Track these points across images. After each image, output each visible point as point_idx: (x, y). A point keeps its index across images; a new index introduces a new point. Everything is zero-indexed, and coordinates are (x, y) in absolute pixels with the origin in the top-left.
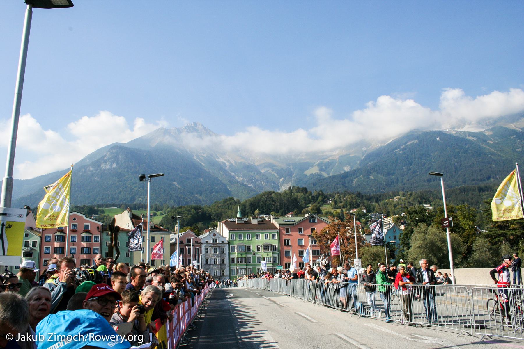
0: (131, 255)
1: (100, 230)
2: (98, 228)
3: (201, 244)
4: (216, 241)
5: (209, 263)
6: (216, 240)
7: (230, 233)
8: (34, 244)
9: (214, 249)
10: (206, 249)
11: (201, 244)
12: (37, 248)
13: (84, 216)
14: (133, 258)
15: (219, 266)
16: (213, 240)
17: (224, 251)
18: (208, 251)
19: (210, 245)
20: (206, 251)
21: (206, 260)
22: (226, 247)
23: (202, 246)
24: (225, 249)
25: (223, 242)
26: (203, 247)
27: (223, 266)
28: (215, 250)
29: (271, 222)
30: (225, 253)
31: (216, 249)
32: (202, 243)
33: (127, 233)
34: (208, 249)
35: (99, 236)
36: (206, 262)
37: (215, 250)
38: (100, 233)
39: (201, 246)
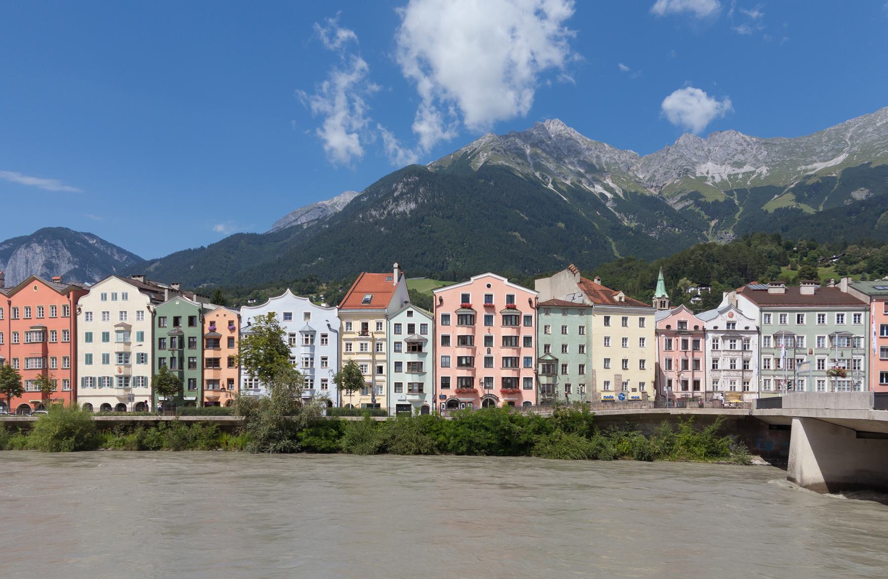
0: (587, 349)
1: (534, 306)
2: (530, 302)
3: (704, 332)
4: (733, 327)
6: (734, 324)
7: (761, 311)
8: (424, 326)
9: (731, 341)
12: (429, 336)
13: (506, 280)
14: (591, 355)
15: (741, 373)
16: (728, 324)
18: (717, 345)
20: (714, 345)
21: (713, 361)
24: (751, 341)
25: (747, 328)
26: (710, 336)
27: (747, 374)
28: (715, 343)
30: (750, 349)
31: (735, 341)
33: (579, 310)
34: (717, 342)
36: (713, 365)
37: (715, 343)
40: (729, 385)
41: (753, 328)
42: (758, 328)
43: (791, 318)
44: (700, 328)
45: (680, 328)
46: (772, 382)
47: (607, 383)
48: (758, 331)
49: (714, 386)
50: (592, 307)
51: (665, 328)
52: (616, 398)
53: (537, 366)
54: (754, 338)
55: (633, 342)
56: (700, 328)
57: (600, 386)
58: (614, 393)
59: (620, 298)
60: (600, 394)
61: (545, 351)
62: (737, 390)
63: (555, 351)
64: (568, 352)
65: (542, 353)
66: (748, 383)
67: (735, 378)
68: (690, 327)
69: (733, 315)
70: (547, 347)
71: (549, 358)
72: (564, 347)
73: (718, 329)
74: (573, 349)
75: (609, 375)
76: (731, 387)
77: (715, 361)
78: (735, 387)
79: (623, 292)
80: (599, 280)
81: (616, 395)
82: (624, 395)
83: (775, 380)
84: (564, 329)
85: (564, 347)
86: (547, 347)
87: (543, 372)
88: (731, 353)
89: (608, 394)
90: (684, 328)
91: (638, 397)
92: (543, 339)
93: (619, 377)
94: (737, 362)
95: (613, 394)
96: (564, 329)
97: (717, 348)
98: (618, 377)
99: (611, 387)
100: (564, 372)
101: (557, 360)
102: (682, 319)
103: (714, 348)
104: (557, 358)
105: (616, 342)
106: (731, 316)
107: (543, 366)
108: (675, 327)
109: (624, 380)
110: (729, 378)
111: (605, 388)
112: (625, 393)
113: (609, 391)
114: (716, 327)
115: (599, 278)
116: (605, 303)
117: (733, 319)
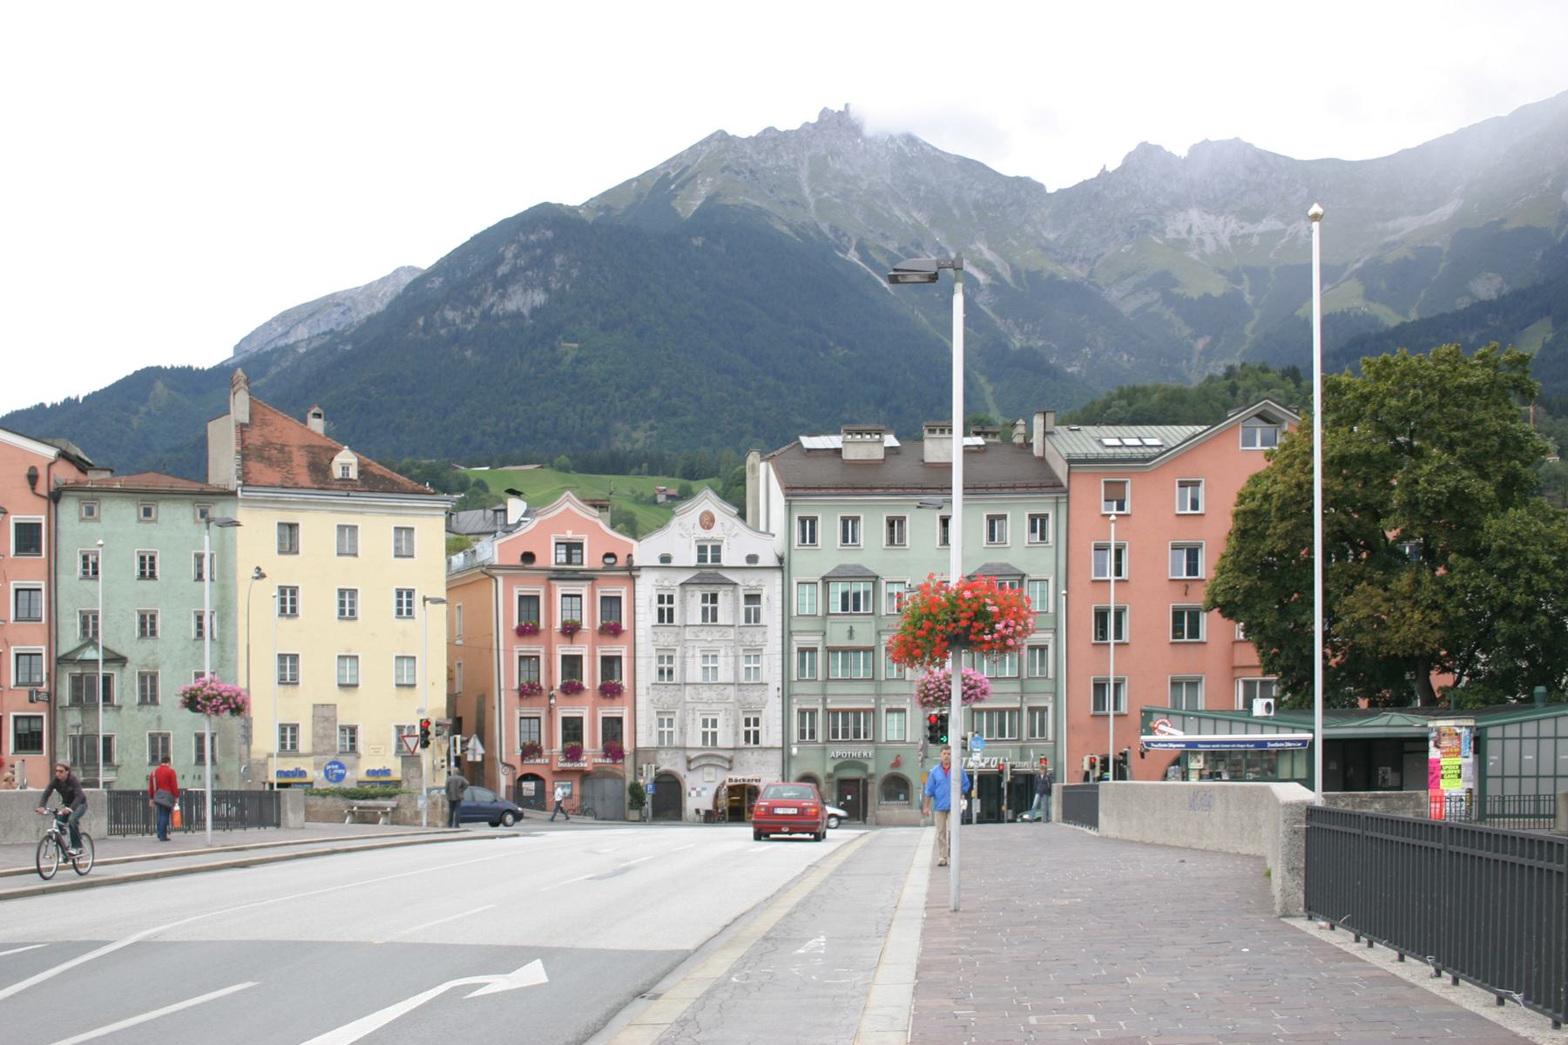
3: (631, 571)
4: (716, 558)
5: (676, 677)
6: (717, 549)
10: (661, 599)
11: (631, 571)
16: (702, 549)
17: (757, 612)
18: (671, 611)
19: (686, 576)
20: (661, 611)
22: (771, 588)
23: (638, 581)
24: (763, 599)
25: (752, 558)
29: (1037, 451)
30: (763, 621)
31: (714, 598)
32: (639, 568)
35: (43, 520)
38: (45, 502)
39: (633, 578)
40: (700, 729)
41: (768, 559)
42: (781, 559)
43: (872, 528)
44: (622, 562)
45: (562, 558)
46: (820, 716)
47: (288, 733)
48: (782, 564)
49: (661, 733)
50: (234, 493)
51: (517, 560)
52: (315, 775)
53: (53, 678)
54: (771, 588)
55: (376, 604)
56: (622, 562)
57: (265, 740)
58: (311, 760)
59: (345, 468)
60: (264, 765)
61: (85, 633)
62: (720, 743)
63: (118, 633)
64: (159, 634)
65: (70, 639)
66: (757, 722)
67: (715, 707)
68: (590, 559)
69: (713, 520)
70: (89, 622)
71: (90, 654)
72: (147, 626)
73: (671, 564)
74: (174, 625)
75: (298, 708)
76: (705, 734)
77: (665, 656)
78: (714, 734)
79: (352, 449)
80: (319, 416)
81: (317, 766)
82: (341, 766)
83: (828, 711)
84: (147, 569)
85: (147, 626)
86: (89, 622)
87: (77, 700)
88: (703, 636)
89: (290, 765)
90: (575, 559)
91: (386, 772)
92: (74, 593)
93: (327, 713)
94: (721, 660)
95: (306, 765)
96: (147, 569)
97: (671, 619)
98: (324, 713)
99: (305, 744)
100: (149, 696)
101: (120, 660)
102: (570, 535)
103: (661, 619)
104: (124, 653)
105: (317, 603)
106: (708, 521)
107: (76, 681)
108: (551, 557)
109: (344, 719)
110: (699, 706)
111: (283, 746)
112: (345, 760)
113: (299, 755)
114: (666, 559)
115: (316, 410)
116: (289, 485)
117: (715, 533)
